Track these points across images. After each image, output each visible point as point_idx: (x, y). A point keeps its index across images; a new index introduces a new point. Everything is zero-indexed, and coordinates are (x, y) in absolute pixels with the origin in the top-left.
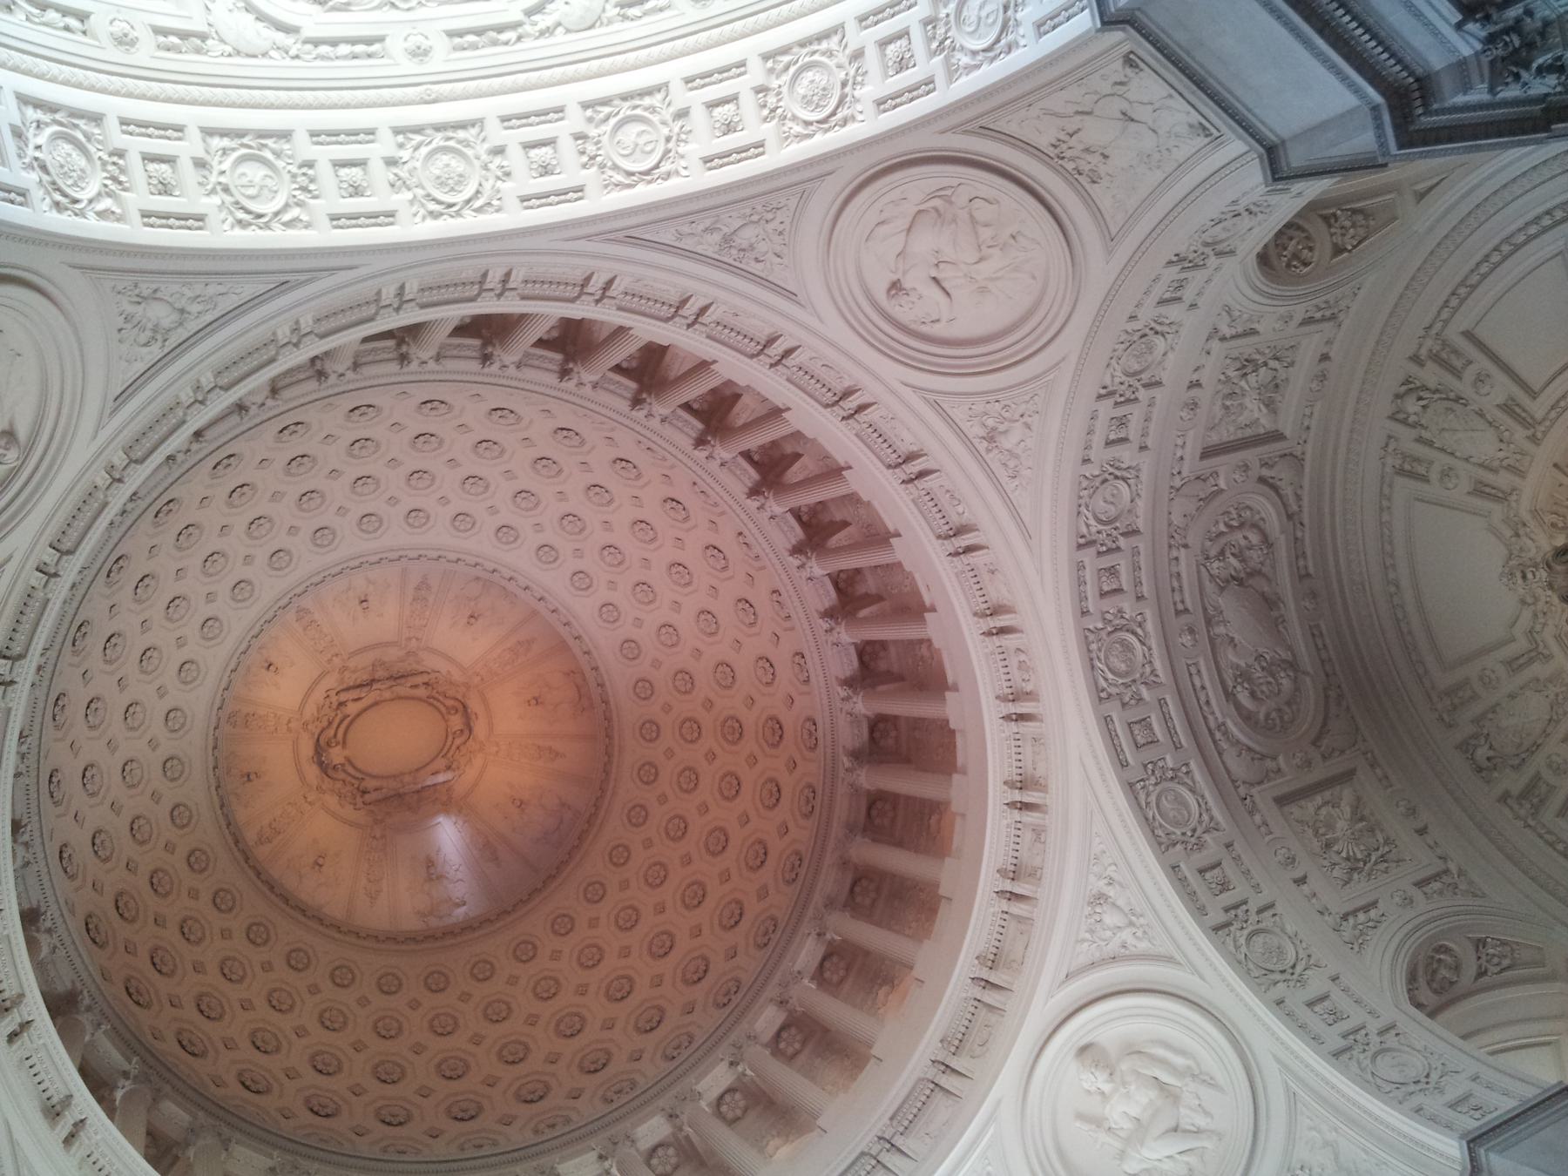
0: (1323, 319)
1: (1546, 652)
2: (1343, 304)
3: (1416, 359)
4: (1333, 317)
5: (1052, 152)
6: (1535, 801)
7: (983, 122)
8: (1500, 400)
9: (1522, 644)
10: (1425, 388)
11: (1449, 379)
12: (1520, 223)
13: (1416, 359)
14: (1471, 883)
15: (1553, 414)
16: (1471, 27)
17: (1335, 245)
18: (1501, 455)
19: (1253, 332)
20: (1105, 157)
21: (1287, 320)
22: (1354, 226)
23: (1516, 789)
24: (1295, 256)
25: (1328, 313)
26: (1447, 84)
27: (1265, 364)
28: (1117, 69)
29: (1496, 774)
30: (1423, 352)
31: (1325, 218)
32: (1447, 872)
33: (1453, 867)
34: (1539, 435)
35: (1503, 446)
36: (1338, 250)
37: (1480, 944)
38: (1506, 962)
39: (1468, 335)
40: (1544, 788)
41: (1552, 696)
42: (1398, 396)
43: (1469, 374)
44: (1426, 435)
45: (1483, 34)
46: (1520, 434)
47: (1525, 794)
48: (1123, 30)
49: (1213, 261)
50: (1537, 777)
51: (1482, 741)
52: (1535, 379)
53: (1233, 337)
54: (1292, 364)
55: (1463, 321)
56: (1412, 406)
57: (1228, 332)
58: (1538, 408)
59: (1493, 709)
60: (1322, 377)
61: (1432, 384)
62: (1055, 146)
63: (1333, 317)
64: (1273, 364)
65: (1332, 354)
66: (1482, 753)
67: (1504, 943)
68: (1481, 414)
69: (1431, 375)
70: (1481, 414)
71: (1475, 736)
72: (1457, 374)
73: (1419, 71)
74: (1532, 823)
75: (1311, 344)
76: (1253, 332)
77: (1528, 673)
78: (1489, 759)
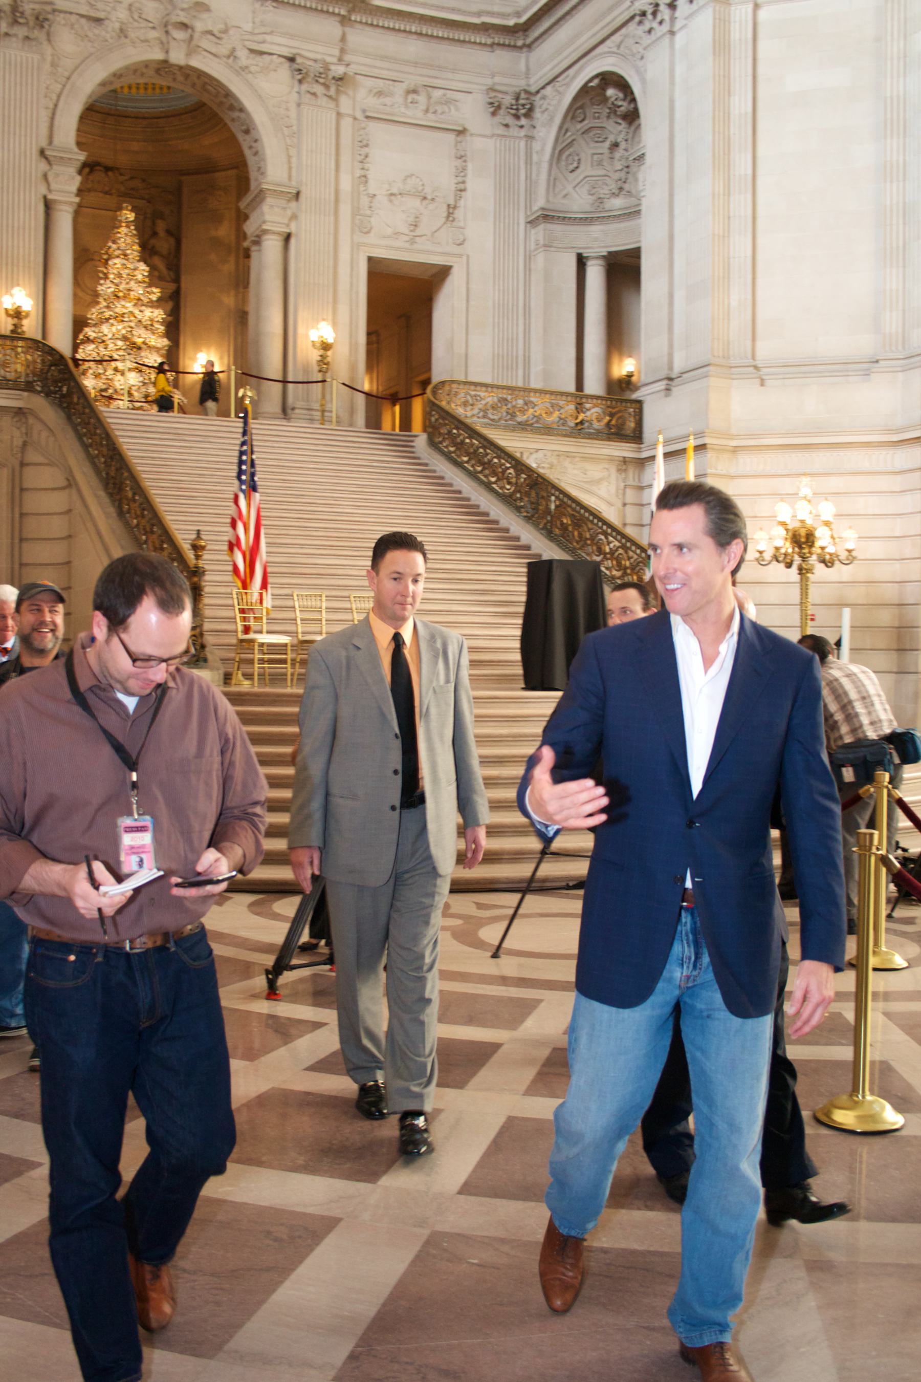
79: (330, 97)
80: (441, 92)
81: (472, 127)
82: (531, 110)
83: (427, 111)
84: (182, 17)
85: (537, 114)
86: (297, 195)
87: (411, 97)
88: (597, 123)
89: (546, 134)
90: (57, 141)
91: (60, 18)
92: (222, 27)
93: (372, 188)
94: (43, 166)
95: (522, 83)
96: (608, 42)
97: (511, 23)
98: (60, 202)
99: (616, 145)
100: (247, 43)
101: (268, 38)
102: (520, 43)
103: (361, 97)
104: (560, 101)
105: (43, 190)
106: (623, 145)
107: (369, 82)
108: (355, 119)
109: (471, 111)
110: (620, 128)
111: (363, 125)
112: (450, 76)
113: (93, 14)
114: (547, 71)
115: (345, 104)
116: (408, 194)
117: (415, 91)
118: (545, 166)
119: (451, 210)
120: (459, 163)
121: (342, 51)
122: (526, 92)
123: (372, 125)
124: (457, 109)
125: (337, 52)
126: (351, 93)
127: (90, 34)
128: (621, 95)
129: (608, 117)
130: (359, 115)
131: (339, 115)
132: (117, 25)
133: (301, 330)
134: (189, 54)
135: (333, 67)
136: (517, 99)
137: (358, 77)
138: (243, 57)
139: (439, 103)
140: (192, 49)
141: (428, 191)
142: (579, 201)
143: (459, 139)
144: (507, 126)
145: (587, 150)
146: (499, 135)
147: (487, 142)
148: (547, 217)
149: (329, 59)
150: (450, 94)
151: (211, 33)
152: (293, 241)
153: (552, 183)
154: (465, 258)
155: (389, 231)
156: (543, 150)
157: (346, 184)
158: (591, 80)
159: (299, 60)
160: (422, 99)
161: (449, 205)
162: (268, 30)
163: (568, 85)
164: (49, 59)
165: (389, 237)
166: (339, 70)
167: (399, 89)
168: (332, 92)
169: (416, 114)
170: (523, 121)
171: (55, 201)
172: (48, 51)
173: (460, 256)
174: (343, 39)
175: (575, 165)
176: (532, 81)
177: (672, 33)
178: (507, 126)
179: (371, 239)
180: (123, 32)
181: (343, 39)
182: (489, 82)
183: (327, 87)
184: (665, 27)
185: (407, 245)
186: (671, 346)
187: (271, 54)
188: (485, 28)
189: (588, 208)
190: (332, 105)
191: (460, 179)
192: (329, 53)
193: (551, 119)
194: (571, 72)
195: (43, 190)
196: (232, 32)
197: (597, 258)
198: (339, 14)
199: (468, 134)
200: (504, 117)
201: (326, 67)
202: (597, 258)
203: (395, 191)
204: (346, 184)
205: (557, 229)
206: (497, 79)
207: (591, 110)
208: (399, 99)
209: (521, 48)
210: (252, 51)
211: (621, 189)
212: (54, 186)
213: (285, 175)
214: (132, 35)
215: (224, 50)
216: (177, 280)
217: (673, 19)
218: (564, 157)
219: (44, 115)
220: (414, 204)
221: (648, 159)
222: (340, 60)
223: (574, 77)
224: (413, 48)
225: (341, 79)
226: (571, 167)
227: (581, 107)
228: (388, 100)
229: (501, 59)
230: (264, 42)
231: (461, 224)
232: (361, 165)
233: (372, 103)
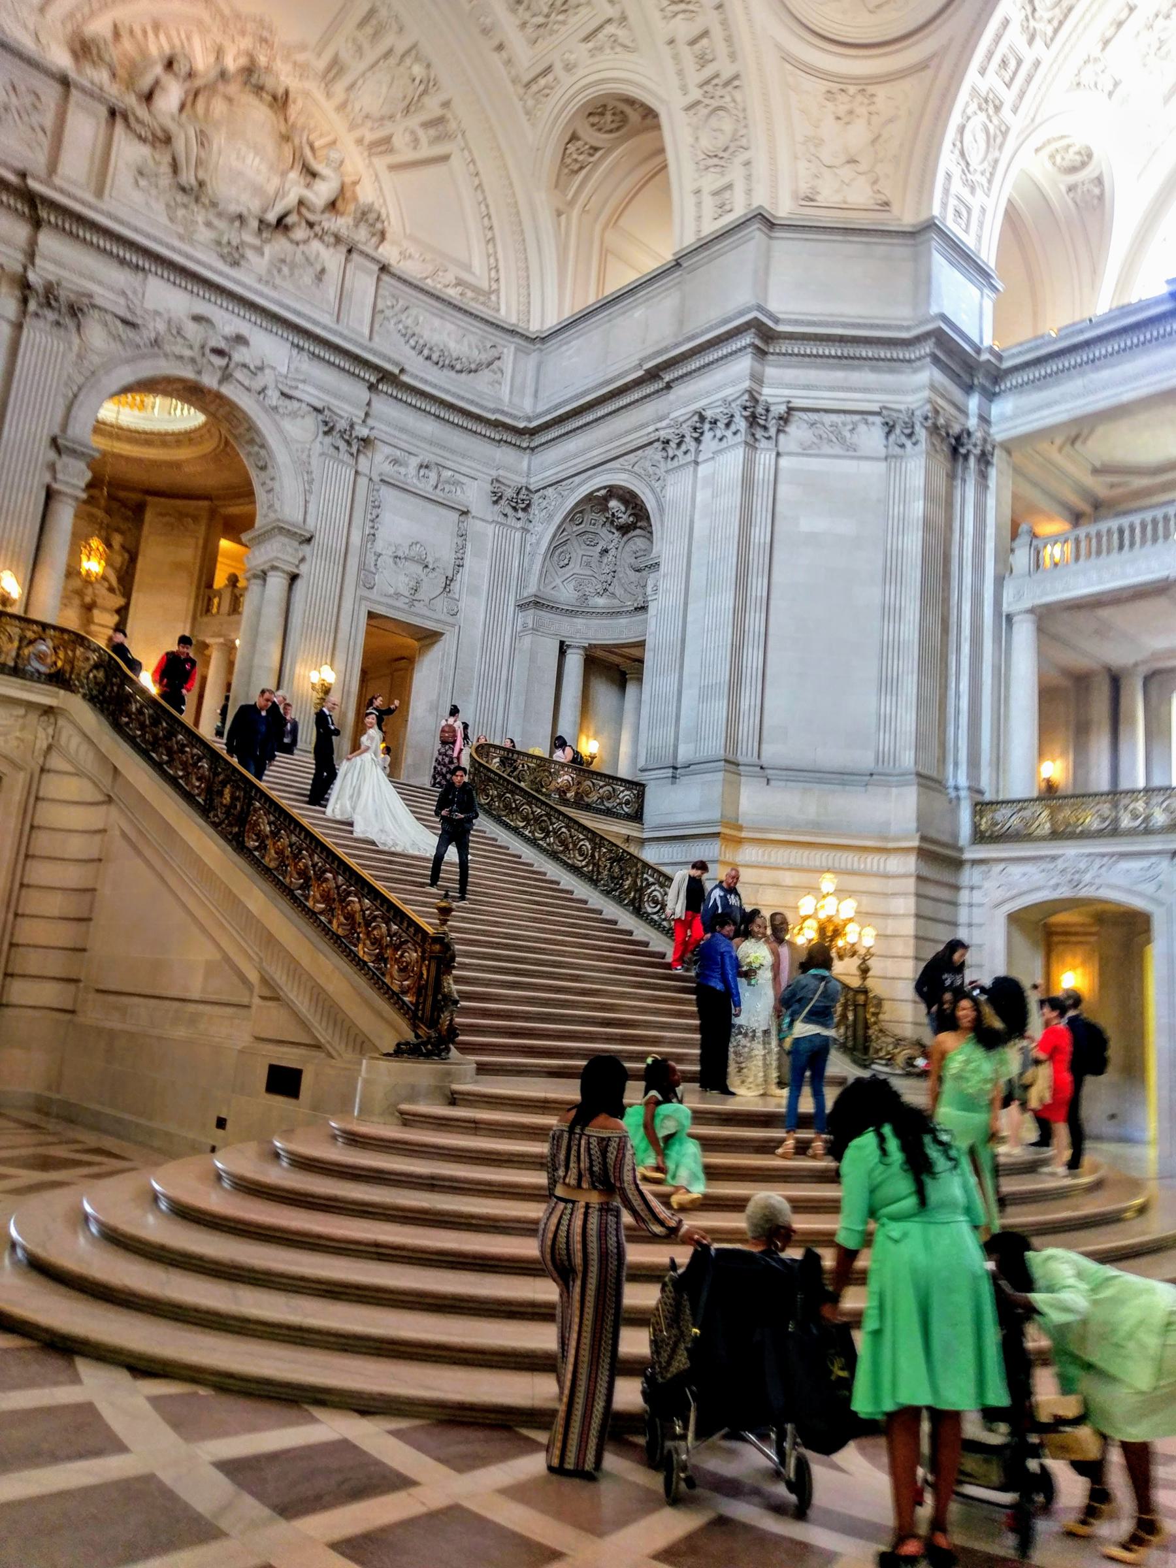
0: (534, 80)
2: (530, 103)
3: (446, 104)
4: (527, 85)
5: (871, 89)
7: (929, 73)
8: (394, 139)
10: (425, 92)
11: (425, 116)
12: (500, 255)
13: (446, 104)
16: (783, 409)
17: (578, 139)
18: (357, 108)
19: (586, 39)
20: (838, 118)
21: (569, 68)
22: (576, 160)
24: (602, 114)
25: (534, 88)
26: (757, 366)
27: (547, 16)
28: (888, 193)
30: (449, 116)
31: (596, 149)
35: (363, 113)
36: (574, 138)
39: (445, 158)
42: (428, 66)
43: (421, 133)
44: (392, 61)
45: (772, 408)
46: (369, 137)
48: (913, 226)
49: (696, 94)
53: (601, 27)
54: (524, 25)
55: (456, 162)
56: (418, 70)
57: (610, 29)
58: (381, 163)
60: (486, 31)
61: (426, 100)
62: (873, 95)
63: (527, 85)
64: (540, 20)
65: (495, 56)
68: (391, 117)
69: (432, 106)
70: (391, 117)
72: (426, 125)
73: (770, 357)
75: (525, 56)
76: (586, 39)
79: (352, 455)
80: (450, 473)
82: (529, 505)
83: (436, 487)
84: (222, 345)
85: (534, 509)
86: (309, 540)
87: (422, 472)
88: (592, 529)
89: (543, 531)
90: (70, 432)
91: (96, 314)
92: (259, 364)
93: (379, 546)
94: (52, 455)
95: (523, 481)
96: (621, 460)
97: (521, 425)
98: (65, 494)
99: (606, 551)
100: (280, 386)
101: (301, 386)
102: (525, 445)
103: (378, 462)
104: (562, 504)
105: (47, 478)
106: (613, 552)
107: (387, 450)
108: (370, 479)
109: (475, 495)
110: (611, 536)
111: (377, 487)
112: (460, 460)
113: (129, 317)
114: (550, 475)
116: (412, 559)
117: (427, 467)
118: (539, 560)
119: (449, 581)
120: (460, 541)
121: (367, 414)
122: (527, 489)
123: (385, 491)
124: (463, 492)
125: (363, 415)
126: (370, 455)
127: (124, 337)
128: (623, 509)
129: (603, 525)
130: (376, 478)
131: (357, 472)
132: (153, 336)
133: (300, 670)
134: (221, 382)
136: (518, 494)
138: (273, 397)
139: (447, 482)
140: (226, 376)
141: (430, 560)
142: (566, 594)
144: (506, 515)
145: (578, 550)
146: (498, 523)
147: (487, 528)
148: (537, 603)
149: (355, 419)
150: (457, 476)
151: (245, 366)
152: (300, 584)
153: (544, 574)
155: (391, 591)
156: (538, 543)
157: (356, 538)
158: (598, 490)
160: (433, 475)
162: (302, 378)
163: (572, 490)
164: (75, 348)
165: (390, 596)
166: (363, 432)
167: (414, 462)
168: (354, 450)
169: (426, 487)
170: (520, 514)
171: (59, 492)
172: (76, 341)
173: (453, 626)
174: (369, 404)
175: (566, 562)
176: (532, 480)
177: (697, 463)
178: (506, 515)
179: (374, 595)
180: (156, 343)
181: (369, 404)
182: (494, 473)
183: (349, 443)
184: (690, 457)
185: (406, 607)
186: (677, 739)
187: (299, 400)
188: (497, 425)
189: (574, 601)
190: (352, 461)
191: (460, 556)
193: (551, 517)
194: (577, 479)
195: (47, 478)
196: (267, 371)
197: (578, 647)
198: (368, 381)
200: (504, 506)
201: (352, 426)
202: (578, 647)
203: (400, 554)
204: (356, 538)
205: (544, 615)
206: (501, 472)
207: (589, 516)
208: (412, 470)
209: (525, 449)
210: (283, 394)
211: (605, 590)
212: (60, 476)
213: (301, 518)
214: (167, 348)
215: (257, 385)
216: (127, 594)
217: (698, 452)
218: (557, 553)
219: (61, 403)
220: (418, 569)
221: (663, 568)
222: (364, 421)
223: (580, 485)
224: (429, 427)
225: (363, 440)
226: (562, 564)
227: (581, 512)
228: (402, 470)
229: (505, 456)
230: (297, 388)
232: (371, 524)
233: (387, 468)
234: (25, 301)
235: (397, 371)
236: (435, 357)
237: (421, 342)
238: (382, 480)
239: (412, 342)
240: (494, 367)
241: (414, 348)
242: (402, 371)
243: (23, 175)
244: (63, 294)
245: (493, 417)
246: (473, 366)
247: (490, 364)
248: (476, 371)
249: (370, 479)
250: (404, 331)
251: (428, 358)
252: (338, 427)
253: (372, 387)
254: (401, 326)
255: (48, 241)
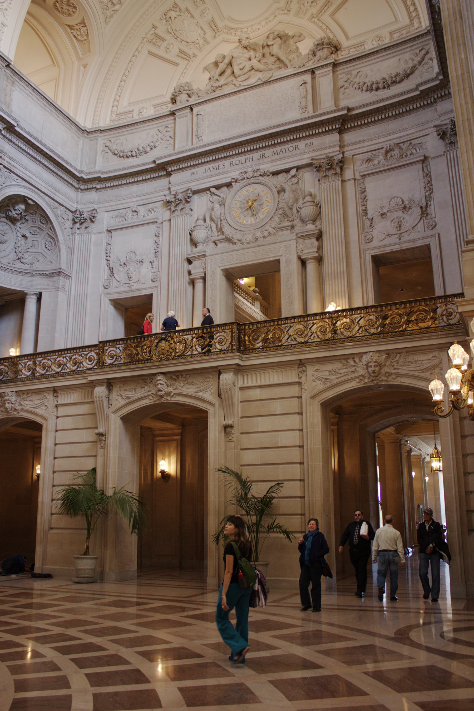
1: (217, 36)
6: (154, 41)
9: (220, 25)
14: (112, 16)
15: (324, 27)
23: (158, 31)
29: (164, 22)
32: (114, 4)
33: (117, 7)
34: (313, 20)
35: (309, 4)
37: (83, 23)
38: (79, 37)
40: (159, 44)
41: (197, 42)
46: (314, 10)
47: (156, 35)
50: (163, 40)
51: (178, 14)
52: (338, 16)
58: (326, 17)
59: (192, 17)
66: (173, 14)
67: (87, 35)
71: (180, 10)
74: (145, 41)
77: (207, 29)
78: (170, 17)
81: (431, 153)
87: (389, 155)
115: (348, 174)
117: (391, 150)
121: (341, 147)
123: (367, 179)
130: (358, 177)
131: (343, 181)
135: (335, 158)
137: (355, 157)
141: (406, 203)
143: (424, 165)
150: (414, 142)
154: (437, 236)
159: (315, 162)
160: (396, 152)
161: (421, 207)
168: (338, 170)
192: (334, 152)
198: (336, 128)
199: (430, 159)
203: (384, 211)
208: (381, 157)
225: (341, 162)
228: (376, 162)
231: (434, 216)
234: (170, 209)
235: (345, 112)
236: (381, 85)
237: (369, 84)
238: (362, 176)
239: (364, 88)
240: (426, 60)
241: (367, 91)
242: (349, 110)
243: (154, 162)
244: (180, 196)
245: (418, 93)
246: (408, 72)
247: (423, 59)
248: (412, 72)
249: (355, 179)
250: (357, 87)
251: (378, 89)
252: (324, 165)
253: (341, 131)
254: (355, 86)
255: (175, 178)
